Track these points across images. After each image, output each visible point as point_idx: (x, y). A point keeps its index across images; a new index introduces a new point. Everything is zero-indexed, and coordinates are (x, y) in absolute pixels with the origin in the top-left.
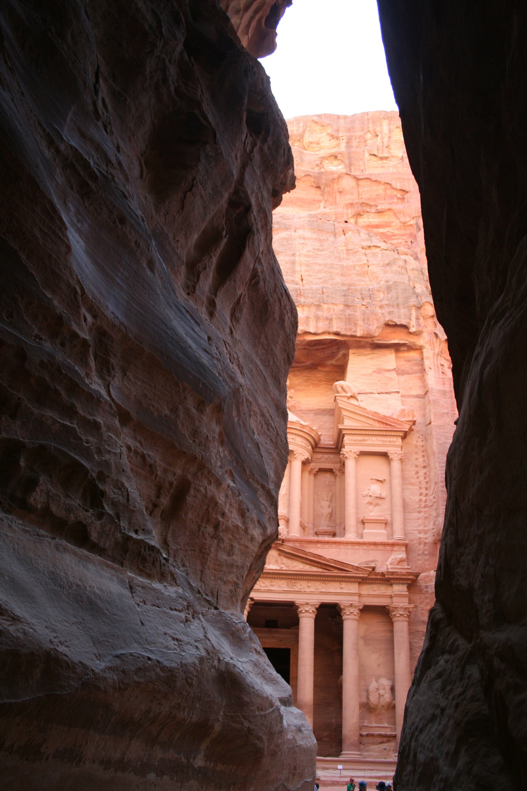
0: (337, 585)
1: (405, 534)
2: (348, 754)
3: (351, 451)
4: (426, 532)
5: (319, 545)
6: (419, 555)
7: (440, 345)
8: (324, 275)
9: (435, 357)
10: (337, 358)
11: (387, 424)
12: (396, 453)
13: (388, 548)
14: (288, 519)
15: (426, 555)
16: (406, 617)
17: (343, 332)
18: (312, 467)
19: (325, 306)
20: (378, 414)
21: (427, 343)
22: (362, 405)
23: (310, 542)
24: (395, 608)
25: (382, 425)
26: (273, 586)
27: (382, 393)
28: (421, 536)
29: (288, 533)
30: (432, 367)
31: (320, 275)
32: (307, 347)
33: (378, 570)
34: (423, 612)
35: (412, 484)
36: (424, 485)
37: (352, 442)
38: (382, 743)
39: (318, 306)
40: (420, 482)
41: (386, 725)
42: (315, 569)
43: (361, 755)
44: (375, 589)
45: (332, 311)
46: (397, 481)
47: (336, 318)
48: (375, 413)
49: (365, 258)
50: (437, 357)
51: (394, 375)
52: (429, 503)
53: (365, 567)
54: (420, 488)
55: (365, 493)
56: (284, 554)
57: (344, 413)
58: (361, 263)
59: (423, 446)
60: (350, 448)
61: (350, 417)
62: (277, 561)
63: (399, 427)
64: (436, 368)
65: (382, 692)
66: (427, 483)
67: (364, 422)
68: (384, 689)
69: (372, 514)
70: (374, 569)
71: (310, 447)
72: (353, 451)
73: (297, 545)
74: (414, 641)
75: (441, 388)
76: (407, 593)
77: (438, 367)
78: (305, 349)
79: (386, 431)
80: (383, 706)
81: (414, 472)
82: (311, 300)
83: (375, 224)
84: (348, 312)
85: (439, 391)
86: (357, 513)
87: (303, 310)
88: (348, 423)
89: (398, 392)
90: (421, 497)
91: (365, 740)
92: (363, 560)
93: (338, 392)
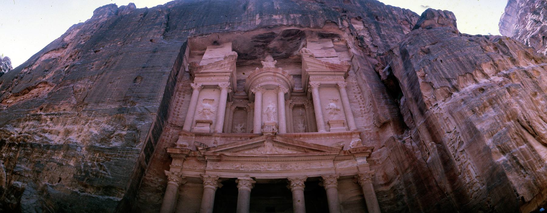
4: (369, 127)
6: (368, 141)
13: (349, 136)
15: (372, 140)
33: (345, 149)
35: (354, 102)
36: (361, 101)
40: (359, 101)
46: (346, 99)
52: (366, 111)
54: (360, 104)
55: (328, 107)
56: (277, 145)
57: (308, 64)
60: (314, 83)
86: (324, 120)
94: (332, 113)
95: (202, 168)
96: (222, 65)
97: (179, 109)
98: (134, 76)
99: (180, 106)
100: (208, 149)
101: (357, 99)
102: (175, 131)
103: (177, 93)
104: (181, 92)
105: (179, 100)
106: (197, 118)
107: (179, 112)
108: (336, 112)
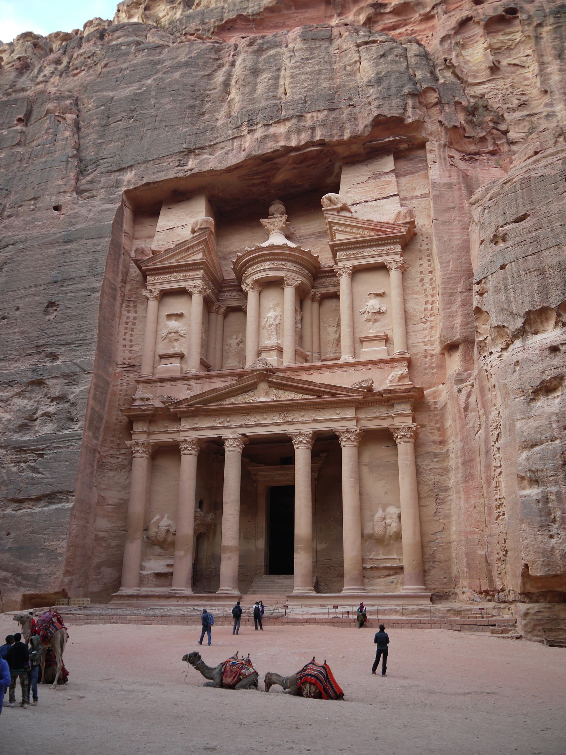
0: (331, 411)
1: (408, 348)
2: (348, 589)
3: (344, 267)
5: (312, 372)
6: (425, 369)
7: (446, 134)
8: (309, 83)
9: (442, 149)
10: (335, 174)
11: (382, 231)
14: (282, 349)
15: (433, 368)
16: (409, 438)
17: (327, 139)
18: (313, 293)
19: (309, 115)
21: (430, 134)
22: (355, 215)
23: (302, 369)
24: (398, 429)
25: (376, 233)
26: (266, 419)
28: (427, 347)
29: (282, 363)
30: (437, 160)
31: (305, 84)
32: (294, 165)
34: (433, 430)
35: (417, 293)
36: (430, 291)
37: (345, 257)
38: (389, 575)
39: (300, 117)
40: (426, 290)
41: (395, 556)
42: (307, 396)
43: (365, 590)
44: (374, 411)
45: (315, 119)
47: (320, 126)
49: (358, 55)
50: (444, 149)
51: (392, 177)
54: (426, 296)
55: (363, 310)
58: (353, 61)
59: (428, 250)
61: (341, 231)
62: (267, 394)
64: (443, 160)
65: (388, 521)
66: (433, 289)
67: (357, 233)
68: (391, 518)
69: (371, 331)
70: (370, 389)
71: (307, 272)
72: (346, 266)
73: (288, 374)
74: (424, 463)
75: (446, 181)
76: (410, 412)
77: (445, 159)
78: (294, 168)
79: (382, 239)
80: (391, 536)
81: (419, 280)
82: (292, 112)
83: (391, 25)
85: (444, 184)
87: (285, 125)
89: (397, 195)
91: (369, 573)
94: (370, 320)
95: (175, 427)
96: (188, 249)
98: (43, 299)
99: (132, 330)
100: (179, 403)
101: (423, 285)
102: (132, 375)
103: (124, 305)
104: (129, 301)
105: (128, 318)
106: (163, 349)
107: (131, 341)
108: (377, 316)
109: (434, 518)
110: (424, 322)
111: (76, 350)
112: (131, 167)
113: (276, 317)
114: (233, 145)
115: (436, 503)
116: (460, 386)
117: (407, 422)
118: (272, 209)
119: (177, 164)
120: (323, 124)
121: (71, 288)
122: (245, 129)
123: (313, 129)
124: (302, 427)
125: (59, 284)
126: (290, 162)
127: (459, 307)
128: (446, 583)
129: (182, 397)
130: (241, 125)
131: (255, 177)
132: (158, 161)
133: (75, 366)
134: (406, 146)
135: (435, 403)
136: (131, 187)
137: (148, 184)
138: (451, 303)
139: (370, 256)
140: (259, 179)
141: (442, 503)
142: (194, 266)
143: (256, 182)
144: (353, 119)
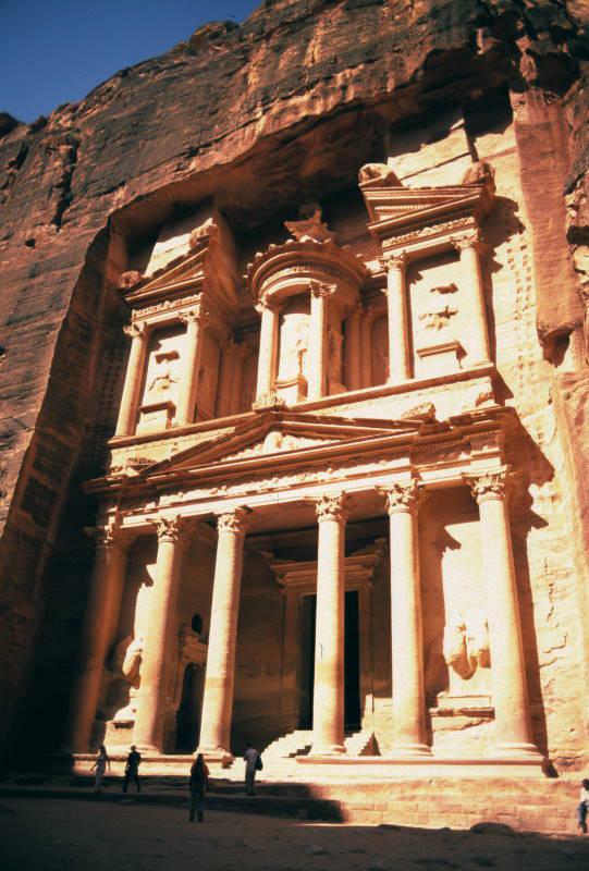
3: (392, 258)
6: (521, 386)
12: (465, 238)
15: (534, 382)
17: (363, 96)
19: (340, 75)
20: (429, 188)
24: (477, 479)
27: (441, 164)
32: (326, 145)
38: (470, 725)
39: (329, 79)
40: (517, 273)
48: (423, 189)
53: (411, 418)
54: (518, 281)
63: (461, 196)
75: (542, 120)
84: (371, 67)
88: (385, 219)
90: (520, 294)
92: (412, 407)
93: (366, 180)
94: (433, 325)
97: (112, 390)
100: (157, 467)
109: (549, 624)
110: (516, 318)
111: (20, 403)
112: (123, 184)
113: (300, 341)
114: (244, 132)
115: (551, 599)
116: (569, 390)
117: (495, 466)
118: (303, 209)
119: (176, 167)
120: (357, 80)
121: (26, 328)
122: (259, 111)
123: (344, 88)
124: (328, 489)
125: (12, 326)
126: (318, 139)
127: (566, 279)
128: (574, 741)
129: (159, 459)
130: (255, 107)
131: (276, 170)
132: (153, 171)
133: (16, 424)
134: (479, 92)
135: (540, 436)
136: (121, 206)
137: (139, 198)
138: (552, 275)
139: (431, 238)
140: (283, 171)
141: (562, 598)
142: (192, 289)
143: (279, 177)
144: (399, 65)
